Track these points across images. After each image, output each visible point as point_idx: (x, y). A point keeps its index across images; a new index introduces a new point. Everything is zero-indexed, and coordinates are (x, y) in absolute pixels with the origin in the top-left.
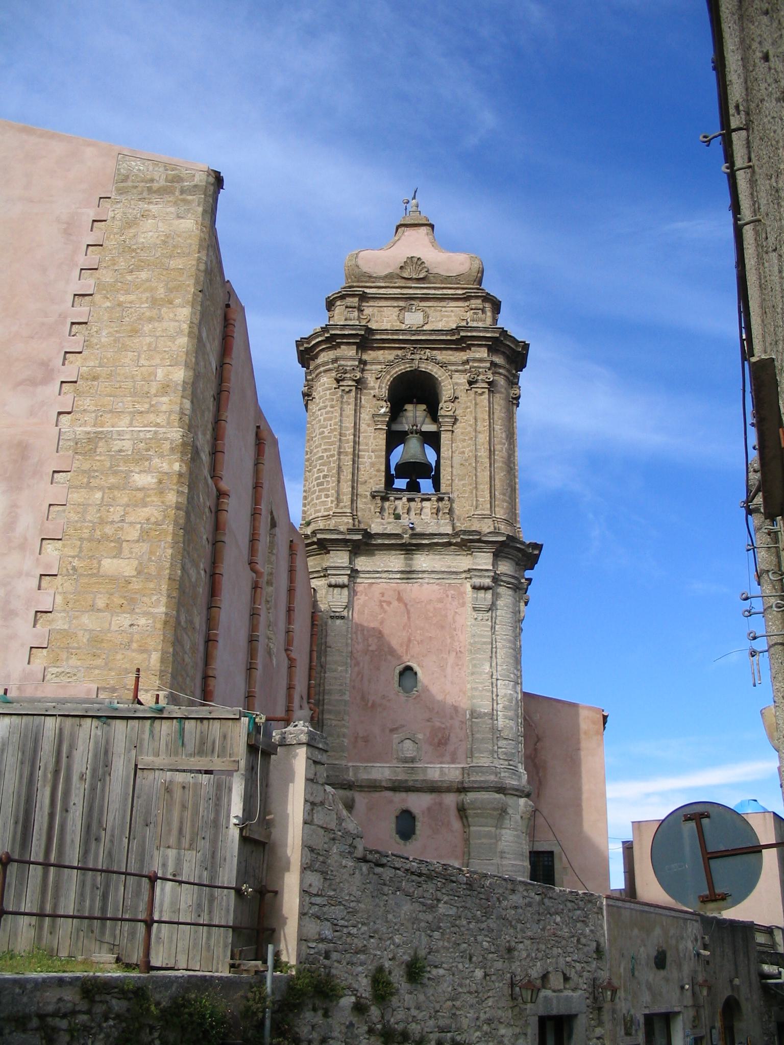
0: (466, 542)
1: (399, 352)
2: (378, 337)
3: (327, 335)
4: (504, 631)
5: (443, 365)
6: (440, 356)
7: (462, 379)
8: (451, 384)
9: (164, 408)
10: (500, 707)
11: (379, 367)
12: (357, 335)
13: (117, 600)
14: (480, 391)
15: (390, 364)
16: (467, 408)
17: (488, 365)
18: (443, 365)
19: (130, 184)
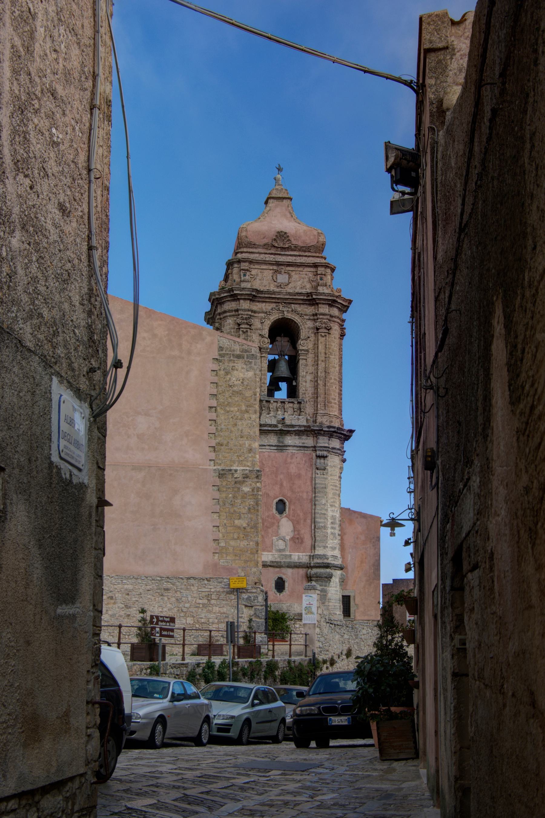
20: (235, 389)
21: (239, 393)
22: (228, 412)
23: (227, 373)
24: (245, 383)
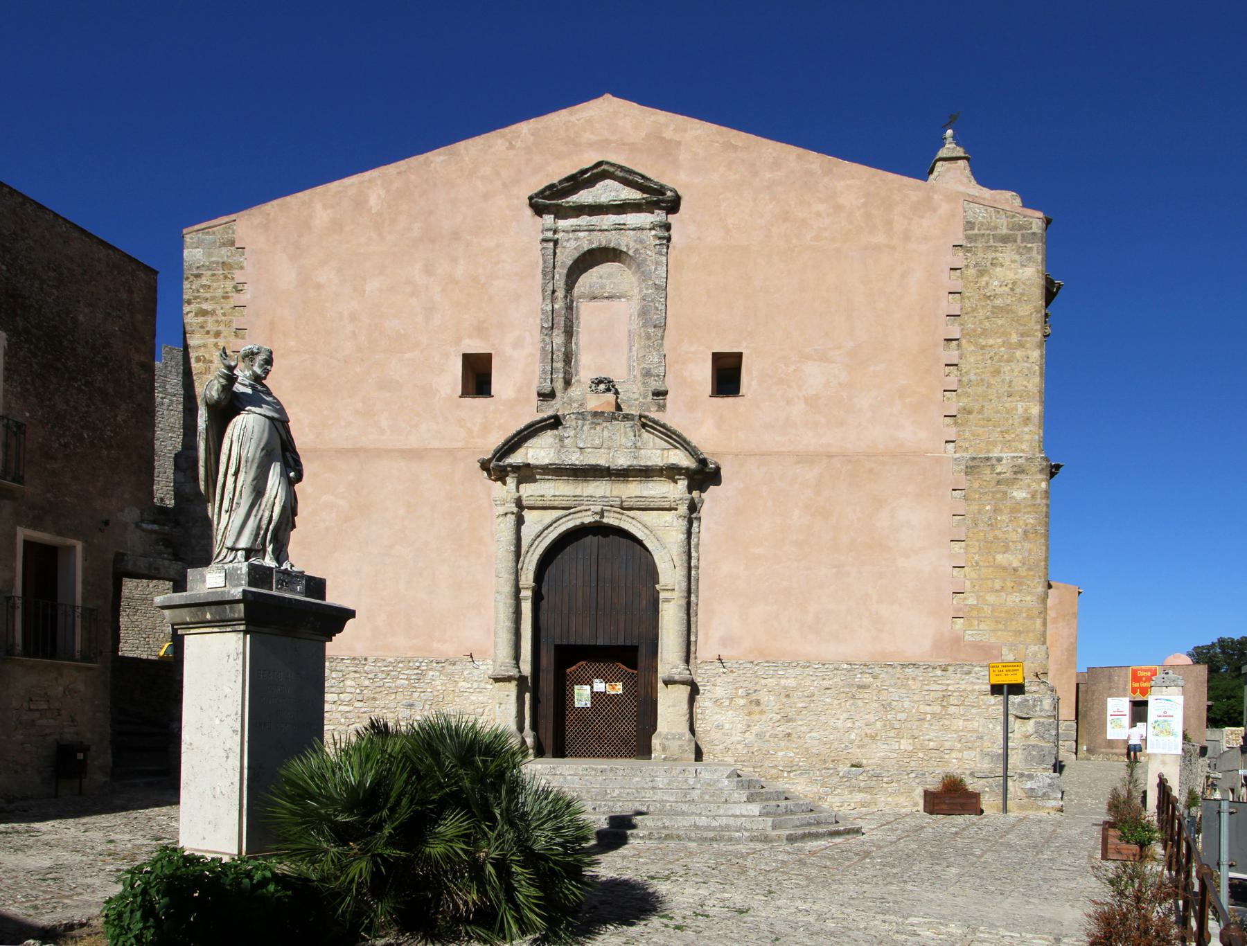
9: (1027, 437)
19: (976, 231)
20: (998, 302)
21: (1006, 309)
22: (983, 348)
23: (982, 273)
24: (1018, 290)
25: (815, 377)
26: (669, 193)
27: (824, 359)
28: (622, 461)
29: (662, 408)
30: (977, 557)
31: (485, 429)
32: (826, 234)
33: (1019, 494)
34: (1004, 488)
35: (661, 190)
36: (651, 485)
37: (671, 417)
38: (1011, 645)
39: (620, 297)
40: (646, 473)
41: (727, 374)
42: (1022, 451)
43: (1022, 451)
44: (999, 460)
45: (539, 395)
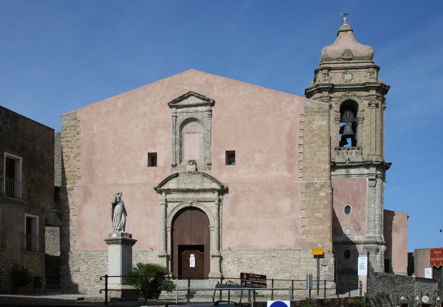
0: (367, 165)
1: (343, 93)
2: (336, 87)
3: (318, 88)
4: (378, 192)
5: (359, 97)
6: (358, 93)
7: (367, 102)
8: (363, 105)
10: (377, 218)
11: (336, 99)
12: (329, 87)
13: (320, 223)
14: (372, 107)
15: (340, 98)
16: (368, 114)
17: (376, 97)
18: (359, 97)
25: (258, 158)
26: (211, 101)
27: (261, 152)
28: (198, 187)
29: (210, 169)
30: (309, 215)
31: (156, 176)
32: (261, 112)
33: (322, 194)
34: (317, 192)
35: (208, 100)
36: (207, 194)
37: (213, 173)
38: (321, 242)
39: (197, 133)
40: (205, 191)
41: (231, 157)
42: (324, 180)
43: (324, 180)
44: (316, 183)
45: (172, 166)
